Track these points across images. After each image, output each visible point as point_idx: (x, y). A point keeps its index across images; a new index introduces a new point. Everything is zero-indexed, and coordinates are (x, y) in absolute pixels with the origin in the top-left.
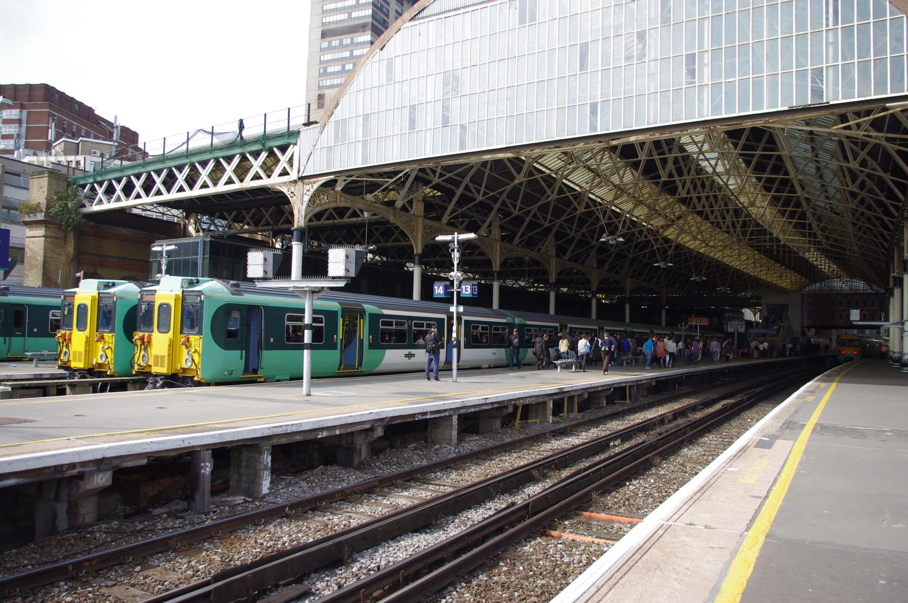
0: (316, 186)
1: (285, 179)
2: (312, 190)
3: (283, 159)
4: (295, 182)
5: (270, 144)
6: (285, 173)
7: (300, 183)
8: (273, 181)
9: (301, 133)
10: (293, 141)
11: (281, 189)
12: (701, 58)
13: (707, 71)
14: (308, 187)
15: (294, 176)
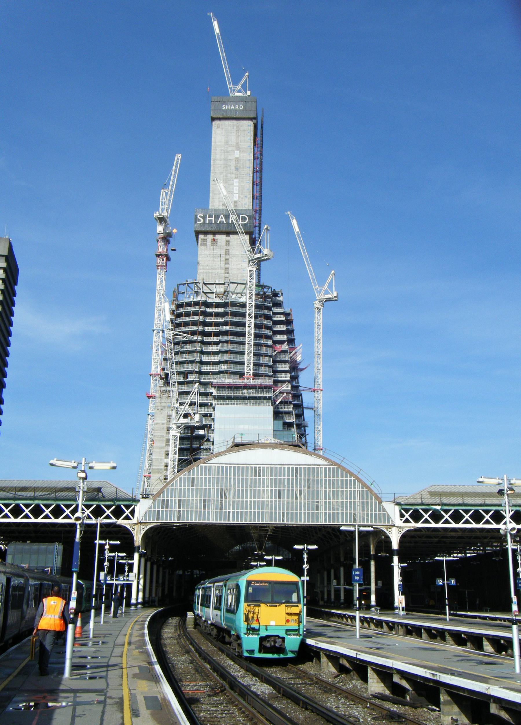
0: (148, 527)
1: (129, 521)
2: (146, 529)
3: (127, 512)
4: (135, 524)
5: (118, 503)
6: (127, 518)
7: (139, 525)
8: (121, 521)
9: (141, 501)
10: (134, 503)
11: (126, 526)
12: (320, 503)
13: (323, 508)
14: (143, 527)
15: (135, 520)
